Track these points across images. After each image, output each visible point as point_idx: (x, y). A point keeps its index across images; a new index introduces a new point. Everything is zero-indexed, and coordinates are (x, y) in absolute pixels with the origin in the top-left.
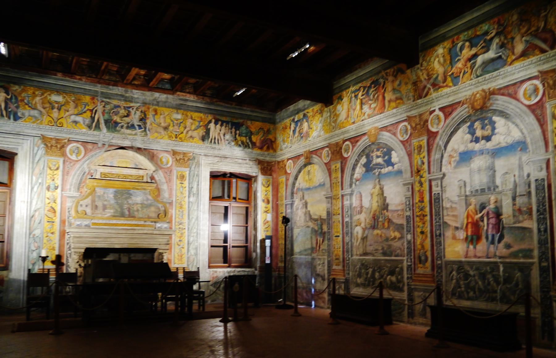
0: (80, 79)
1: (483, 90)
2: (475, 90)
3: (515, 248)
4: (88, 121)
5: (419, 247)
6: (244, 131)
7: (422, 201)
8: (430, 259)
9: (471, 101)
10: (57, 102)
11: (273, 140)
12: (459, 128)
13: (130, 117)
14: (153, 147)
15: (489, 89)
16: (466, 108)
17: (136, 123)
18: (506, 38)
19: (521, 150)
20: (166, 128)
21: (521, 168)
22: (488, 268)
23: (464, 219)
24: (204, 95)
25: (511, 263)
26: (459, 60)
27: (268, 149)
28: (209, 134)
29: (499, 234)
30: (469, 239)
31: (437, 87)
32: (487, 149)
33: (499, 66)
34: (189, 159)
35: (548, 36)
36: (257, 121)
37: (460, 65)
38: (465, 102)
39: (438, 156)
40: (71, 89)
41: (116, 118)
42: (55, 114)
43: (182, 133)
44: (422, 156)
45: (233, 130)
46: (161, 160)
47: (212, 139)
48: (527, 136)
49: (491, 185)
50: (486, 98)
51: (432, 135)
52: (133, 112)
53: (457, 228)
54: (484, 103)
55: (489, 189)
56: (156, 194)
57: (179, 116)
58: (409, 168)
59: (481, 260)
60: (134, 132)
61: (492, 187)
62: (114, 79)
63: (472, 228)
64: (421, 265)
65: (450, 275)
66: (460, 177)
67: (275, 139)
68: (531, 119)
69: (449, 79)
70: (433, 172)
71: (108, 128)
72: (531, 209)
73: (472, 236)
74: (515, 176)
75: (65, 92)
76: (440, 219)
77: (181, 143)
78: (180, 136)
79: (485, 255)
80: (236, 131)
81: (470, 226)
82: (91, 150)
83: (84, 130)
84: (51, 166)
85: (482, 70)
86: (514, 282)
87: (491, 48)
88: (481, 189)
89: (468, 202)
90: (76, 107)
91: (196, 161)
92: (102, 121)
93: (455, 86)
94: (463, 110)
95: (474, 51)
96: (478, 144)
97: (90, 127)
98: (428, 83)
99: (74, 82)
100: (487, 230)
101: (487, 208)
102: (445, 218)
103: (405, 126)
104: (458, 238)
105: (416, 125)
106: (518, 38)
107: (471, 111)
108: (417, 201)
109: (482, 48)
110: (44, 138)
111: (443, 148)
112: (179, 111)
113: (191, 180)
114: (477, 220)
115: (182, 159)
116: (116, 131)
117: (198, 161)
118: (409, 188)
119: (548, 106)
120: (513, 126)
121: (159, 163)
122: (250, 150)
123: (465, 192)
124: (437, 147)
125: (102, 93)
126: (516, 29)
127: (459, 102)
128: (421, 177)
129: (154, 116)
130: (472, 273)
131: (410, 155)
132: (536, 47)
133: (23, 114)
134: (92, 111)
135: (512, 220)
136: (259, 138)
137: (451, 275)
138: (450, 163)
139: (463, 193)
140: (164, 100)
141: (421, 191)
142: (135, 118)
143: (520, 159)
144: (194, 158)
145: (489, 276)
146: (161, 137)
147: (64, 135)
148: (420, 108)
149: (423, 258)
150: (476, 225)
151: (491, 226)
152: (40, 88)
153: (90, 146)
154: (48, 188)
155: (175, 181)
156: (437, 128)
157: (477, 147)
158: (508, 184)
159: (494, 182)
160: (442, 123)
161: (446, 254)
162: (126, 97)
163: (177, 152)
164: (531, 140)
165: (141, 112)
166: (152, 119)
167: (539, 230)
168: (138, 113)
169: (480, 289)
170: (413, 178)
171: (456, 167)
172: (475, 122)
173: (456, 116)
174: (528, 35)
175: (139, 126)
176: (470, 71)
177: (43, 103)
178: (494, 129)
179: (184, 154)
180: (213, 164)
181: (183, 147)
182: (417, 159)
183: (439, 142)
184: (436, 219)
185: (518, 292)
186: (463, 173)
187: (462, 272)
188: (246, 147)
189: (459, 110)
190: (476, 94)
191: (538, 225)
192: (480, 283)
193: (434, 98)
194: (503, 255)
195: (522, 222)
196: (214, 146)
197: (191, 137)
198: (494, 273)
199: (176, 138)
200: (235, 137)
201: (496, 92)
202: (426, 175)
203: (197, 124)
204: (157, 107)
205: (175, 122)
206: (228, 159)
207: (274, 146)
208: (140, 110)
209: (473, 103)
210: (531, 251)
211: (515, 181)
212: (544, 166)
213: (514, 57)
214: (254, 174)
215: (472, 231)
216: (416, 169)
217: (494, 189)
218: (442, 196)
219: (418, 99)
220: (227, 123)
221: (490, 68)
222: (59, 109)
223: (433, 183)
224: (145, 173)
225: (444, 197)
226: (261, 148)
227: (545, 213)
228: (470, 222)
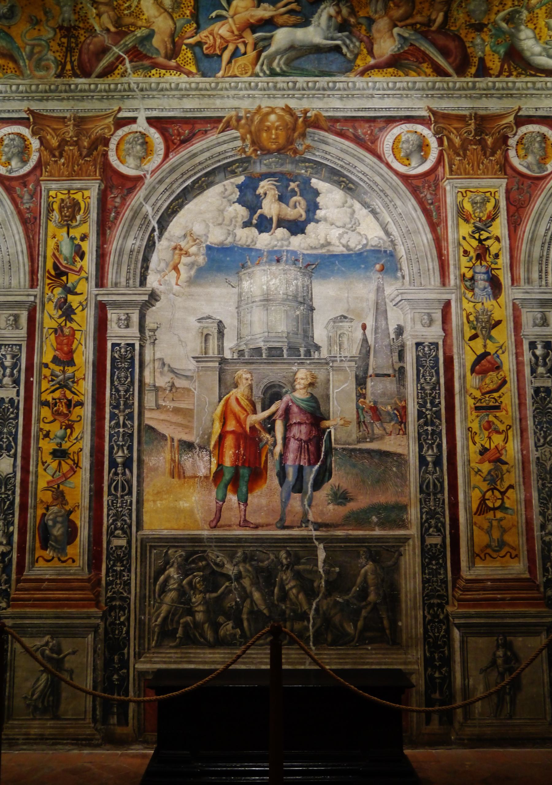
1: (288, 110)
2: (266, 104)
3: (362, 501)
5: (48, 497)
7: (66, 359)
8: (84, 534)
9: (252, 127)
12: (210, 184)
15: (306, 112)
16: (235, 139)
18: (353, 12)
19: (382, 270)
21: (380, 310)
22: (283, 554)
23: (213, 421)
25: (347, 539)
26: (220, 18)
29: (317, 467)
30: (227, 476)
31: (146, 63)
32: (294, 253)
33: (334, 68)
35: (452, 45)
37: (223, 30)
38: (234, 122)
39: (134, 242)
44: (76, 233)
48: (399, 241)
49: (299, 340)
50: (294, 129)
51: (117, 186)
53: (188, 446)
54: (290, 141)
55: (293, 350)
58: (23, 260)
59: (260, 532)
61: (301, 346)
63: (237, 447)
64: (49, 553)
65: (156, 579)
66: (207, 310)
68: (409, 206)
69: (186, 54)
70: (116, 285)
72: (405, 408)
73: (236, 468)
74: (364, 327)
76: (130, 417)
79: (274, 519)
81: (229, 441)
85: (287, 64)
86: (356, 589)
87: (314, 20)
88: (270, 349)
89: (228, 378)
93: (204, 75)
94: (225, 142)
95: (265, 12)
96: (265, 236)
98: (116, 44)
100: (283, 456)
101: (285, 399)
102: (147, 414)
103: (19, 135)
104: (188, 473)
105: (63, 143)
106: (382, 24)
107: (249, 150)
108: (48, 358)
109: (291, 12)
111: (154, 223)
114: (253, 428)
118: (16, 318)
119: (448, 188)
120: (365, 211)
123: (221, 349)
124: (134, 218)
126: (380, 5)
127: (219, 120)
128: (71, 291)
130: (230, 569)
131: (30, 223)
132: (425, 58)
135: (353, 432)
137: (162, 578)
138: (176, 268)
139: (213, 350)
141: (67, 331)
143: (379, 290)
145: (286, 576)
148: (82, 99)
149: (57, 531)
150: (250, 443)
151: (293, 445)
156: (138, 168)
157: (263, 241)
158: (345, 345)
159: (307, 334)
160: (157, 159)
161: (146, 518)
164: (408, 252)
167: (422, 460)
169: (255, 614)
170: (37, 291)
171: (191, 282)
172: (261, 180)
173: (202, 152)
174: (406, 26)
176: (252, 54)
178: (313, 207)
182: (57, 240)
183: (141, 206)
184: (113, 416)
185: (364, 613)
186: (218, 300)
187: (199, 570)
189: (213, 138)
190: (268, 114)
191: (421, 447)
192: (257, 595)
193: (133, 86)
194: (327, 519)
195: (381, 438)
198: (301, 567)
201: (323, 123)
202: (87, 288)
209: (259, 131)
210: (403, 508)
211: (365, 340)
212: (438, 316)
213: (372, 62)
215: (237, 456)
216: (50, 265)
217: (308, 353)
218: (141, 354)
219: (76, 76)
221: (307, 63)
223: (112, 315)
225: (148, 357)
227: (437, 421)
228: (233, 432)
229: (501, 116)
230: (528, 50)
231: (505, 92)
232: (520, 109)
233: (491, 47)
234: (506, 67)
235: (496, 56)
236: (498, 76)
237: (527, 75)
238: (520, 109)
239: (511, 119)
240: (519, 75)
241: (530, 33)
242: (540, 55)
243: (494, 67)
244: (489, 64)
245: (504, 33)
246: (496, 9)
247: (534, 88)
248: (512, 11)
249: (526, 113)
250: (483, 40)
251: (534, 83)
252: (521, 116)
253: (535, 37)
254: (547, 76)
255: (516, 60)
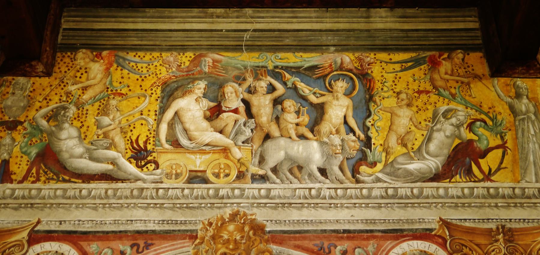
229: (11, 232)
230: (67, 151)
231: (25, 201)
232: (39, 222)
233: (21, 148)
234: (34, 171)
235: (25, 158)
236: (21, 182)
237: (58, 181)
238: (39, 222)
239: (24, 235)
240: (49, 179)
241: (74, 132)
242: (81, 157)
243: (17, 171)
244: (13, 168)
245: (42, 131)
246: (38, 104)
247: (64, 197)
248: (57, 108)
249: (47, 228)
250: (14, 140)
251: (65, 190)
252: (38, 231)
253: (79, 137)
254: (83, 182)
255: (50, 162)
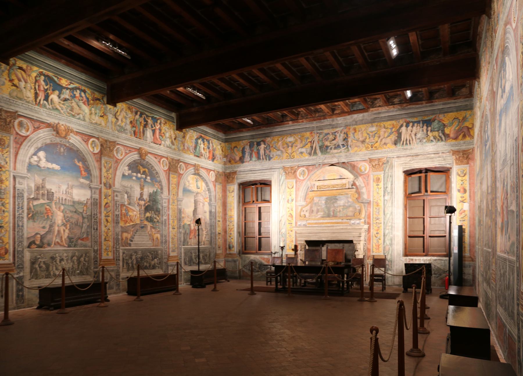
0: (302, 122)
4: (309, 150)
6: (437, 126)
10: (290, 142)
11: (470, 127)
13: (337, 140)
14: (354, 159)
17: (341, 143)
20: (363, 142)
24: (393, 104)
27: (464, 136)
28: (401, 138)
34: (383, 164)
36: (451, 112)
40: (298, 131)
41: (327, 143)
42: (290, 150)
43: (377, 142)
45: (425, 127)
46: (360, 169)
47: (403, 142)
52: (338, 135)
56: (357, 196)
57: (374, 129)
60: (339, 151)
62: (321, 114)
67: (473, 124)
71: (322, 152)
75: (295, 134)
77: (376, 151)
78: (375, 145)
80: (427, 127)
82: (312, 171)
83: (307, 157)
84: (289, 186)
90: (301, 142)
91: (389, 164)
92: (318, 148)
97: (310, 154)
99: (300, 125)
110: (284, 168)
112: (374, 124)
113: (386, 181)
115: (378, 164)
116: (327, 152)
117: (392, 164)
121: (359, 171)
122: (443, 143)
125: (317, 127)
129: (353, 134)
133: (273, 155)
134: (311, 142)
136: (453, 128)
140: (361, 119)
142: (340, 140)
144: (388, 162)
146: (359, 150)
147: (295, 164)
152: (280, 135)
153: (311, 168)
154: (288, 201)
155: (372, 184)
162: (333, 125)
163: (373, 160)
165: (344, 133)
166: (352, 137)
168: (342, 135)
175: (343, 145)
177: (283, 145)
179: (379, 159)
180: (406, 163)
181: (377, 155)
188: (439, 140)
196: (405, 147)
197: (385, 144)
199: (372, 147)
200: (427, 134)
203: (389, 131)
204: (356, 126)
205: (371, 134)
206: (420, 156)
207: (471, 133)
208: (343, 132)
214: (448, 166)
220: (418, 122)
222: (292, 147)
224: (347, 182)
226: (456, 138)
